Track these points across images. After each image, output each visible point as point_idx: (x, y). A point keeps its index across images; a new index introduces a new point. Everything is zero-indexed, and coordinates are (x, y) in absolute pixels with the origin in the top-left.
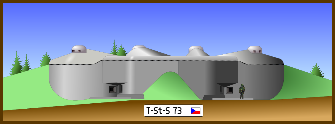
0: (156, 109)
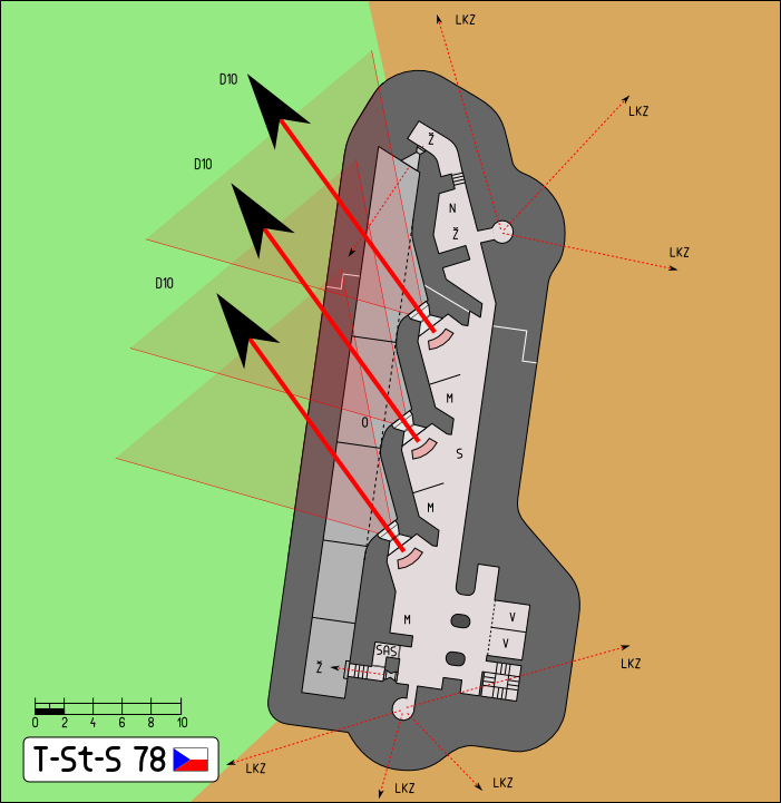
0: (68, 753)
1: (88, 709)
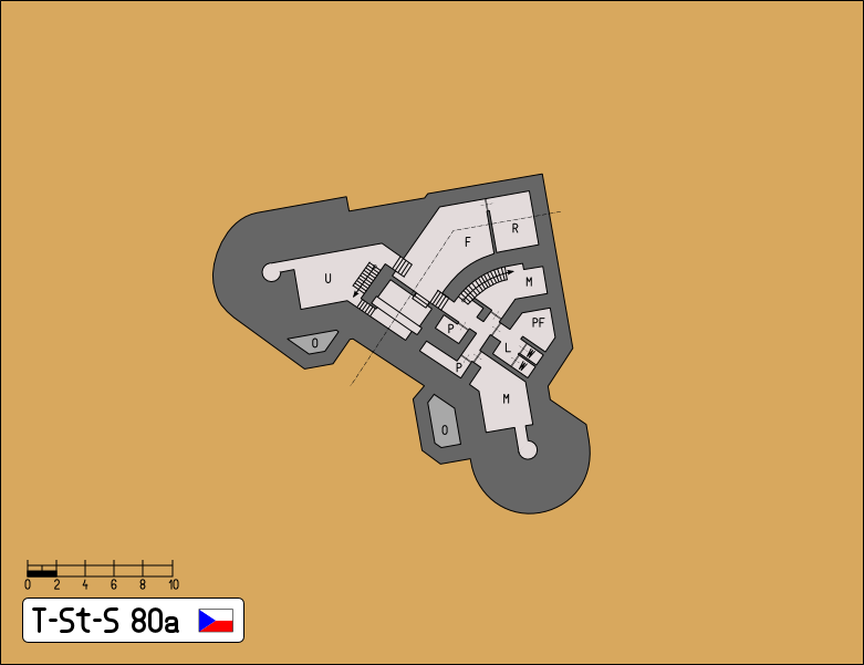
0: (67, 615)
1: (80, 571)
